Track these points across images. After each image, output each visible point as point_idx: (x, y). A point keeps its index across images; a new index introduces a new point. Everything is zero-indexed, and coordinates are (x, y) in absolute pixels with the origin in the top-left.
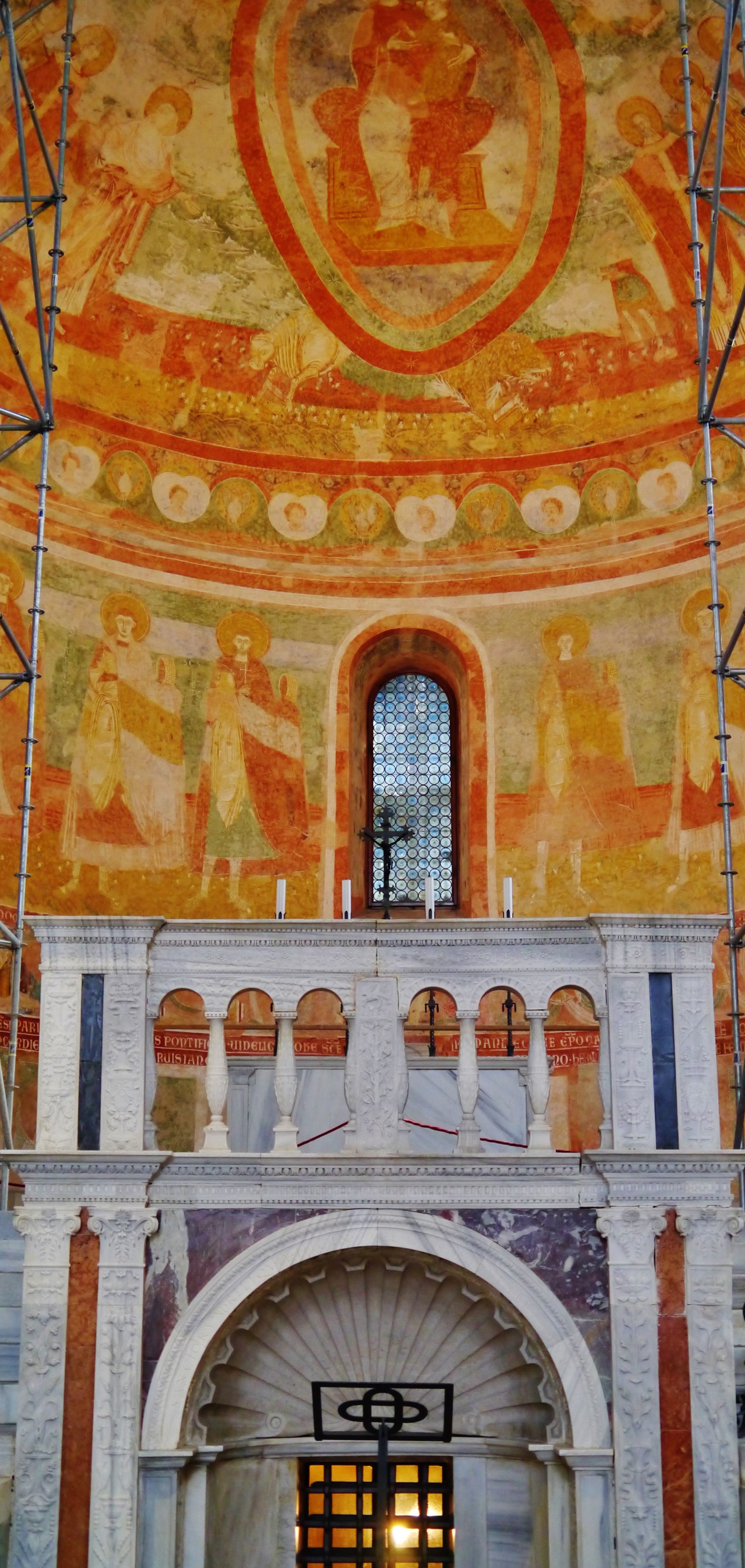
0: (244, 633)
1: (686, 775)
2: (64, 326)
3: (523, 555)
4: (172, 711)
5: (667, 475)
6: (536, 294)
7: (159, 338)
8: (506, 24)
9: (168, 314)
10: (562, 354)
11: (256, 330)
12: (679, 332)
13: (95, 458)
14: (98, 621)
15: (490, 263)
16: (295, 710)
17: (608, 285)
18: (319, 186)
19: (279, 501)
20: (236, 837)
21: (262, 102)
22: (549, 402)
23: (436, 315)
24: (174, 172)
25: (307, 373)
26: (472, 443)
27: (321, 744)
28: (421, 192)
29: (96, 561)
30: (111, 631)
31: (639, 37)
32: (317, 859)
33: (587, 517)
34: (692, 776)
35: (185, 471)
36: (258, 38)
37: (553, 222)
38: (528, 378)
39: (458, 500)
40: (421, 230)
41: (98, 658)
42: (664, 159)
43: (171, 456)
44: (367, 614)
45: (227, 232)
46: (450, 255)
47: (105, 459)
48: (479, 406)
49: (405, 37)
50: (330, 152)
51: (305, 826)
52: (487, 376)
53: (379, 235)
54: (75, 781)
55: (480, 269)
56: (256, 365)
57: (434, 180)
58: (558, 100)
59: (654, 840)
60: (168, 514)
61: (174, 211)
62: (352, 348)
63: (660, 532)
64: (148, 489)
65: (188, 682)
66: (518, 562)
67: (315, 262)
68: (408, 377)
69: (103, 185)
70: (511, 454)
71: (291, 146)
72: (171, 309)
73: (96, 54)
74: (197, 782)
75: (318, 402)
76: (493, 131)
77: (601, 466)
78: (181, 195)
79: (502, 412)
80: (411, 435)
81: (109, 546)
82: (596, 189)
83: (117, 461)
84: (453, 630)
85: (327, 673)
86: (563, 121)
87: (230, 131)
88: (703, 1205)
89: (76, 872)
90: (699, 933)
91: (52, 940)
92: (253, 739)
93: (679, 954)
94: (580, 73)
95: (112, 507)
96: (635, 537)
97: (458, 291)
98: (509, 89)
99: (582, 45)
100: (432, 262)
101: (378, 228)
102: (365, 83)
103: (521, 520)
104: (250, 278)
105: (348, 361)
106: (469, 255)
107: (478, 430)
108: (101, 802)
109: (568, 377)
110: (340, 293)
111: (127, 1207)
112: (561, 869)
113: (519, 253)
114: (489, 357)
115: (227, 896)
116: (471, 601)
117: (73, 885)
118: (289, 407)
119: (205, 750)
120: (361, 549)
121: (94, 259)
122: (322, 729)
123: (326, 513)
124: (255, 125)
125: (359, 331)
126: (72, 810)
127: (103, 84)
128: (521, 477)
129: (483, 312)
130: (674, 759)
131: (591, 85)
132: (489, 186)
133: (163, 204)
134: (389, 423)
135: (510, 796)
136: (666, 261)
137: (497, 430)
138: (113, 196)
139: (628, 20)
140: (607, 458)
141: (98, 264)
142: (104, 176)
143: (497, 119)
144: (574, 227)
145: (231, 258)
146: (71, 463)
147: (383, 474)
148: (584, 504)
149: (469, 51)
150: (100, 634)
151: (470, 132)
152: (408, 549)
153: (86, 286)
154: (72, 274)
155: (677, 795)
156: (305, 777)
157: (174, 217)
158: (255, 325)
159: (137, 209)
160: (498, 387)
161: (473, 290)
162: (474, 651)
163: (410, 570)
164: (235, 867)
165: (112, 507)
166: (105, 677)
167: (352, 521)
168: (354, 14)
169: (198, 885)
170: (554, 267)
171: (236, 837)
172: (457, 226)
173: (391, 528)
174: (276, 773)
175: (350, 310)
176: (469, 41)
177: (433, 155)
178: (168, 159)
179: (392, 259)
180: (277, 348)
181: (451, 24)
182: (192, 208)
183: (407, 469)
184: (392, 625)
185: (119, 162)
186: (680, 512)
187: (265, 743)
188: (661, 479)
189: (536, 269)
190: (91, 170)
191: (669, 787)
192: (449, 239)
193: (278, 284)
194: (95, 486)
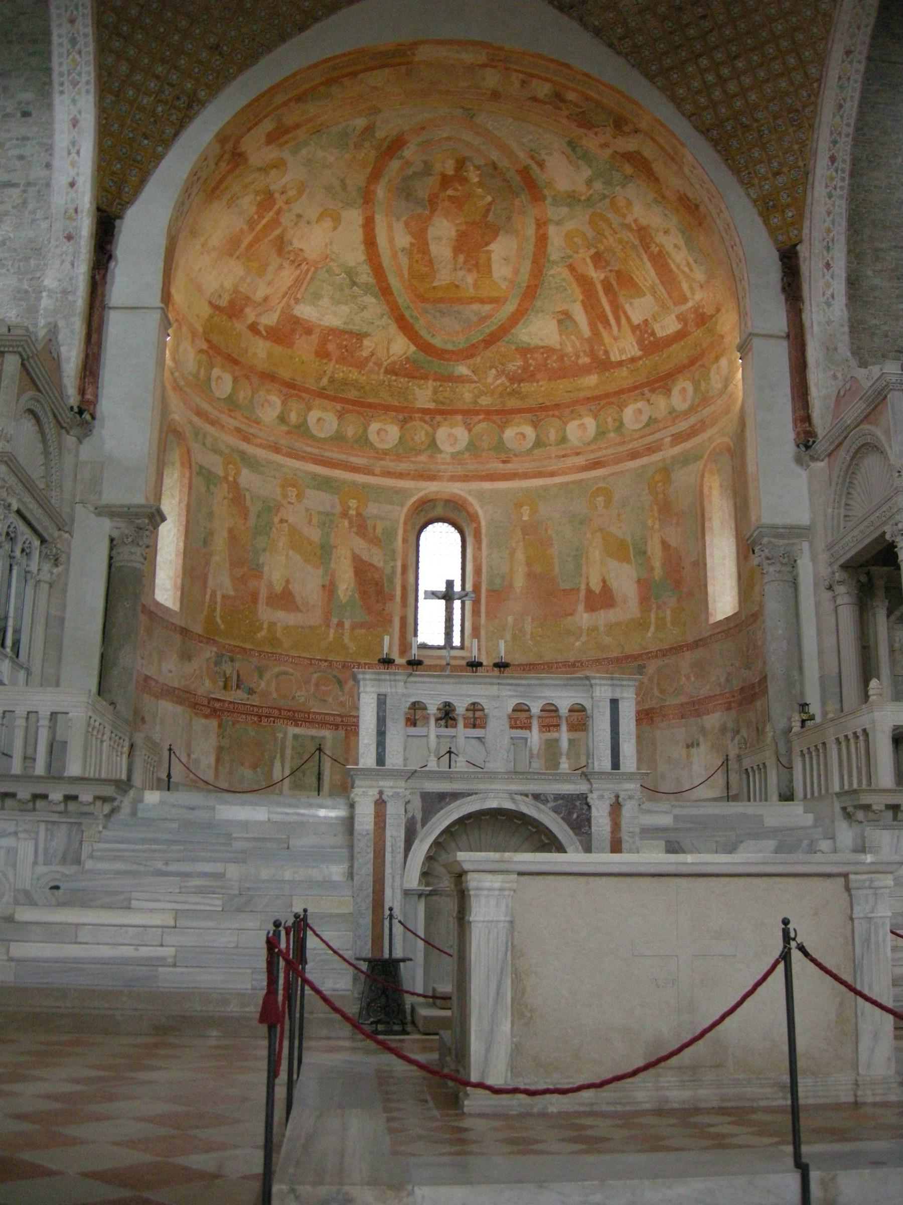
0: (354, 498)
1: (588, 584)
2: (266, 332)
3: (504, 462)
4: (316, 540)
5: (583, 424)
6: (517, 323)
7: (315, 338)
8: (510, 187)
9: (320, 325)
10: (529, 356)
11: (366, 335)
12: (592, 351)
13: (278, 402)
14: (278, 490)
15: (493, 305)
16: (380, 541)
17: (555, 322)
18: (404, 261)
19: (374, 427)
20: (348, 609)
21: (379, 218)
22: (521, 381)
23: (462, 331)
24: (328, 252)
25: (392, 359)
26: (479, 401)
27: (394, 560)
28: (458, 267)
29: (279, 458)
30: (285, 496)
31: (579, 200)
32: (391, 621)
33: (538, 443)
34: (591, 584)
35: (325, 409)
36: (379, 187)
37: (528, 287)
38: (511, 367)
39: (470, 430)
40: (457, 286)
41: (278, 510)
42: (589, 261)
43: (318, 401)
44: (419, 490)
45: (354, 283)
46: (472, 300)
47: (284, 403)
48: (483, 381)
49: (456, 190)
50: (412, 244)
51: (384, 604)
52: (488, 365)
53: (434, 288)
54: (265, 577)
55: (487, 308)
56: (365, 354)
57: (465, 262)
58: (534, 227)
59: (569, 618)
60: (315, 433)
61: (327, 271)
62: (417, 347)
63: (578, 454)
64: (306, 420)
65: (324, 524)
66: (501, 466)
67: (400, 301)
68: (446, 363)
69: (292, 258)
70: (499, 407)
71: (391, 240)
72: (322, 323)
73: (295, 192)
74: (329, 578)
75: (397, 374)
76: (499, 238)
77: (548, 416)
78: (332, 264)
79: (496, 384)
80: (446, 394)
81: (284, 451)
82: (552, 272)
83: (289, 404)
84: (466, 500)
85: (397, 521)
86: (536, 237)
87: (360, 231)
88: (629, 793)
89: (265, 626)
90: (630, 683)
91: (364, 679)
92: (358, 556)
93: (622, 692)
94: (546, 214)
95: (285, 428)
96: (564, 456)
97: (475, 319)
98: (509, 218)
99: (549, 200)
100: (462, 304)
101: (434, 284)
102: (433, 211)
103: (503, 443)
104: (365, 307)
105: (414, 353)
106: (482, 301)
107: (482, 393)
108: (278, 588)
109: (532, 368)
110: (412, 317)
111: (398, 790)
112: (520, 631)
113: (508, 303)
114: (490, 354)
115: (343, 640)
116: (475, 485)
117: (264, 633)
118: (382, 377)
119: (332, 562)
120: (416, 455)
121: (284, 296)
122: (394, 551)
123: (399, 435)
124: (373, 229)
125: (421, 337)
126: (263, 593)
127: (297, 208)
128: (504, 420)
129: (488, 331)
130: (581, 575)
131: (552, 220)
132: (495, 267)
133: (322, 268)
134: (434, 387)
135: (495, 591)
136: (586, 312)
137: (492, 393)
138: (296, 264)
139: (574, 191)
140: (551, 413)
141: (285, 299)
142: (292, 254)
143: (501, 232)
144: (538, 291)
145: (355, 297)
146: (266, 404)
147: (430, 414)
148: (537, 436)
149: (489, 199)
150: (279, 498)
151: (487, 239)
152: (443, 455)
153: (279, 310)
154: (272, 304)
155: (582, 594)
156: (385, 578)
157: (326, 275)
158: (366, 332)
159: (308, 270)
160: (494, 371)
161: (483, 319)
162: (476, 513)
163: (443, 467)
164: (347, 624)
165: (285, 428)
166: (281, 521)
167: (413, 439)
168: (430, 177)
169: (328, 634)
170: (527, 310)
171: (348, 609)
172: (476, 286)
174: (369, 574)
175: (417, 327)
176: (489, 193)
177: (466, 249)
178: (326, 245)
179: (441, 300)
180: (376, 345)
181: (480, 185)
182: (337, 271)
184: (432, 497)
185: (300, 246)
186: (589, 444)
187: (364, 558)
188: (579, 425)
189: (517, 310)
190: (286, 250)
191: (578, 590)
192: (472, 292)
193: (379, 311)
194: (278, 417)
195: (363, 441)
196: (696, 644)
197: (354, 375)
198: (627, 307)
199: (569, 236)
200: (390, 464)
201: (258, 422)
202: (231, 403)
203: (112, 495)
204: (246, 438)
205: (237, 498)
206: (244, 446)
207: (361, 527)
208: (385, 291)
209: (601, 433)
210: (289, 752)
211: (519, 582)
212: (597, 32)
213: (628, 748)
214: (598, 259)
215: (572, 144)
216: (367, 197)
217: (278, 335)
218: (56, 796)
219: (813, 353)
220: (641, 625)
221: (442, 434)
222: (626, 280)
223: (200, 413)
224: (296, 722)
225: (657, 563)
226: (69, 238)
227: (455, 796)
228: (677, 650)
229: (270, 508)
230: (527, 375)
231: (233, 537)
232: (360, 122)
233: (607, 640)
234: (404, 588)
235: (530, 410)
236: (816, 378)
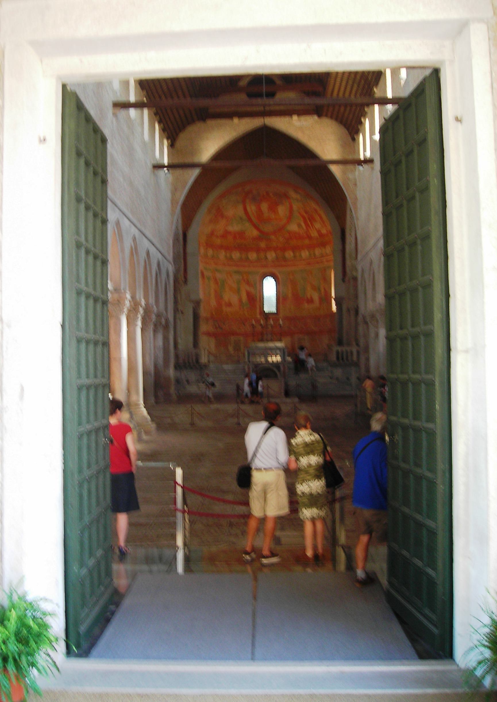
33: (295, 257)
173: (266, 258)
195: (247, 259)
198: (314, 224)
205: (216, 280)
207: (248, 283)
208: (250, 220)
211: (290, 295)
214: (306, 212)
216: (244, 203)
219: (347, 256)
225: (323, 294)
231: (216, 292)
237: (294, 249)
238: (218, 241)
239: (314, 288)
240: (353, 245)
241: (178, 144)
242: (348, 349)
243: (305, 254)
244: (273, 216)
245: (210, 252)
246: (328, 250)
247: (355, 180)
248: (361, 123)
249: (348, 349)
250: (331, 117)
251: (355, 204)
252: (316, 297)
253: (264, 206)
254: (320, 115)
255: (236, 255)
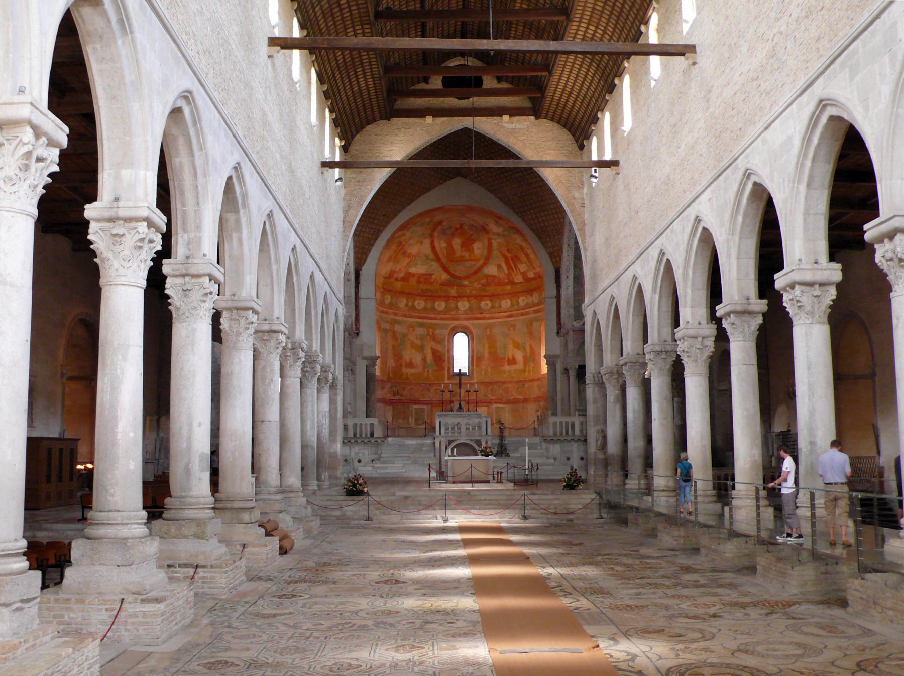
3: (481, 313)
7: (416, 278)
18: (445, 251)
19: (437, 303)
29: (405, 319)
33: (492, 307)
45: (428, 259)
47: (407, 300)
55: (473, 263)
106: (471, 261)
108: (408, 361)
116: (471, 322)
126: (404, 364)
173: (457, 307)
183: (459, 296)
195: (433, 309)
196: (539, 380)
197: (429, 287)
199: (499, 244)
200: (443, 316)
201: (399, 308)
202: (391, 305)
203: (366, 353)
204: (396, 314)
205: (394, 333)
206: (396, 317)
207: (434, 338)
208: (438, 259)
209: (512, 305)
210: (414, 414)
211: (486, 355)
212: (500, 199)
213: (489, 430)
214: (508, 250)
215: (496, 222)
216: (432, 236)
217: (404, 279)
218: (373, 441)
220: (524, 371)
221: (460, 304)
222: (518, 258)
223: (383, 312)
224: (416, 404)
225: (528, 351)
226: (348, 280)
227: (455, 440)
228: (533, 381)
229: (404, 336)
230: (488, 284)
231: (394, 347)
232: (428, 220)
233: (514, 375)
234: (449, 358)
235: (489, 296)
236: (563, 312)
237: (493, 296)
238: (399, 285)
239: (518, 346)
240: (571, 290)
241: (353, 148)
242: (569, 419)
243: (506, 303)
244: (467, 255)
245: (388, 299)
246: (535, 298)
247: (583, 199)
248: (595, 120)
249: (569, 419)
250: (552, 120)
251: (582, 229)
252: (519, 356)
253: (457, 242)
254: (537, 119)
255: (420, 303)
